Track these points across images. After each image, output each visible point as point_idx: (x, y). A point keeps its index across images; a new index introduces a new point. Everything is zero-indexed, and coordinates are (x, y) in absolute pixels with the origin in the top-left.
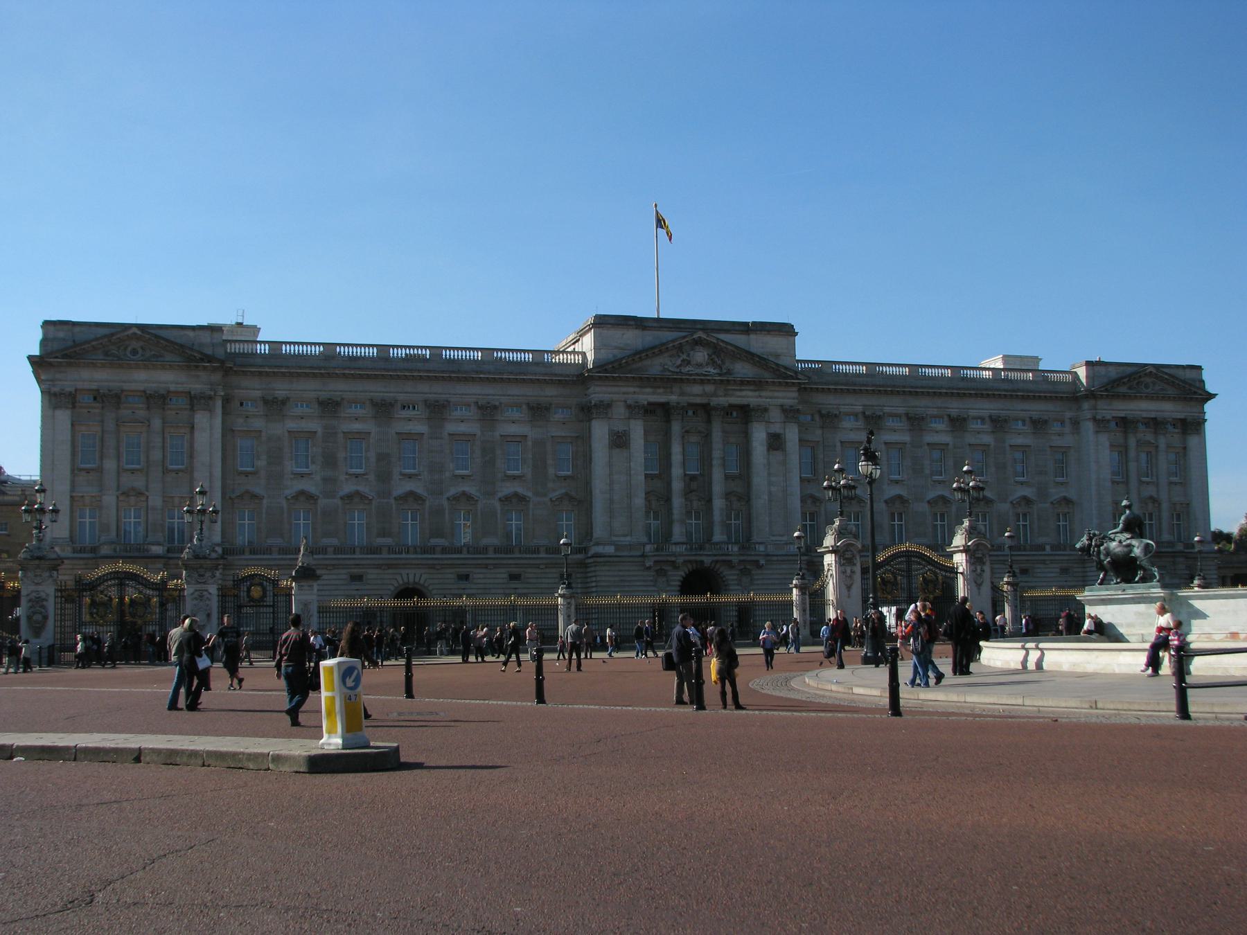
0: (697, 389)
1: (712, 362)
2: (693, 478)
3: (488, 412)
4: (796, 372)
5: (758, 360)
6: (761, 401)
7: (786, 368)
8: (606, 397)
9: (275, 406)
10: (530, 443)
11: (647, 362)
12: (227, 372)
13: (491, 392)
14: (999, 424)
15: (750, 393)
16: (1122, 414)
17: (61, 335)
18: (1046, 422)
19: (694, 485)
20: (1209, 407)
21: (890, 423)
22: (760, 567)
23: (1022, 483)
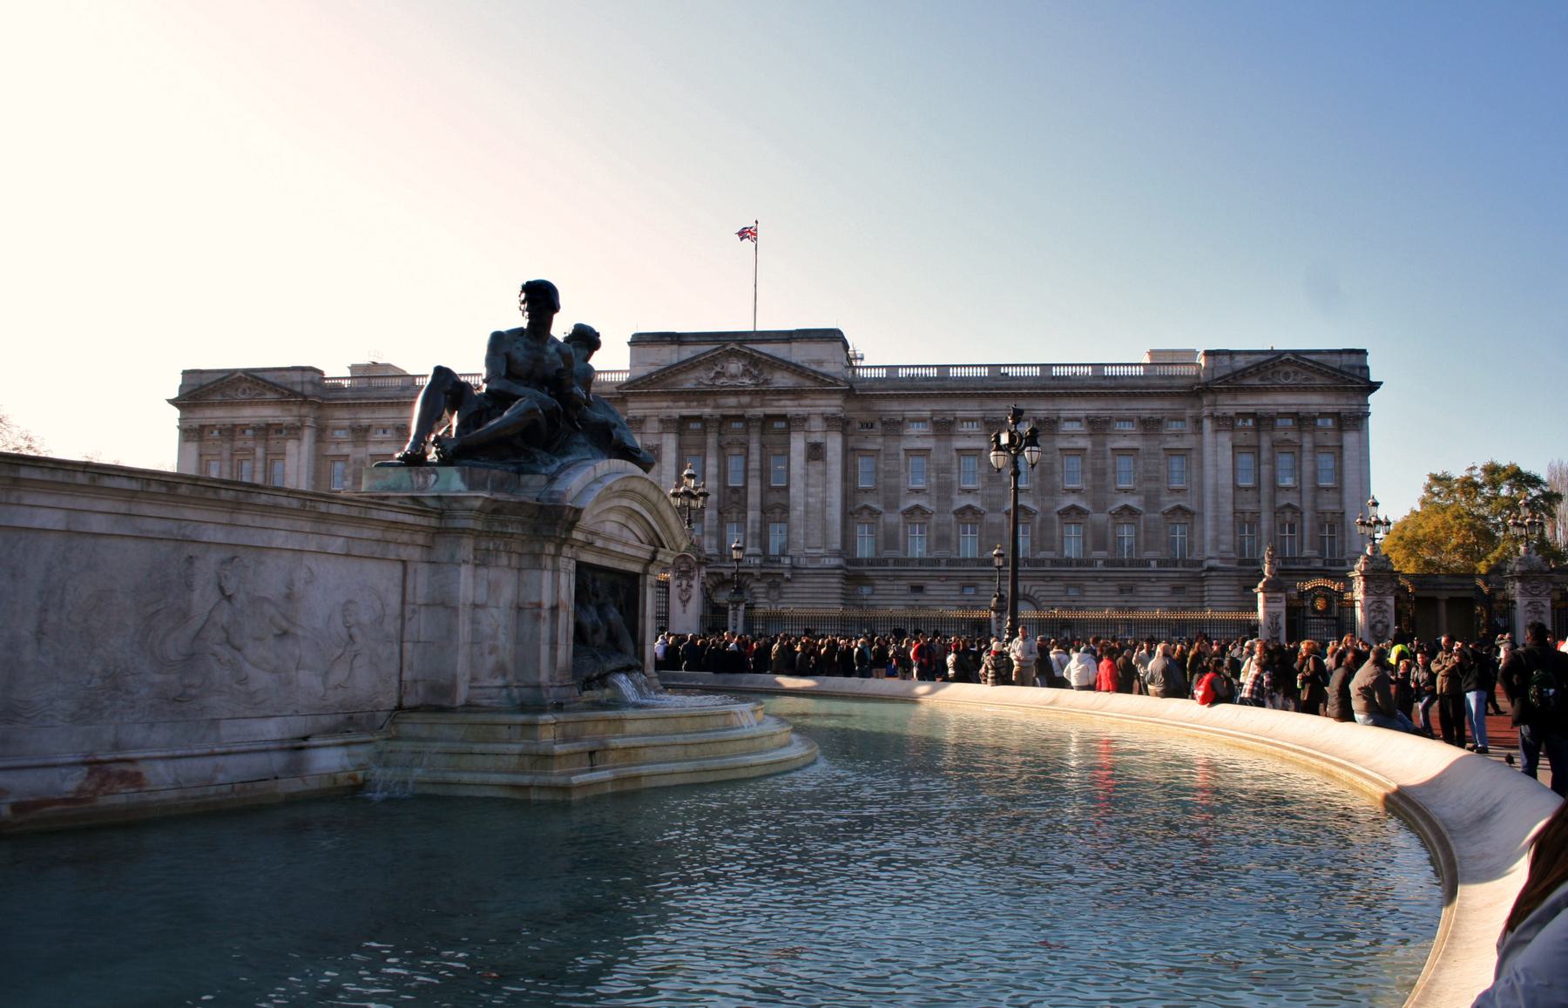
0: (732, 401)
1: (746, 373)
2: (735, 490)
6: (802, 411)
7: (824, 375)
8: (639, 413)
9: (360, 433)
11: (682, 377)
12: (320, 406)
15: (788, 403)
17: (194, 381)
18: (1159, 422)
19: (735, 498)
20: (1372, 398)
21: (966, 428)
22: (788, 580)
23: (1126, 491)
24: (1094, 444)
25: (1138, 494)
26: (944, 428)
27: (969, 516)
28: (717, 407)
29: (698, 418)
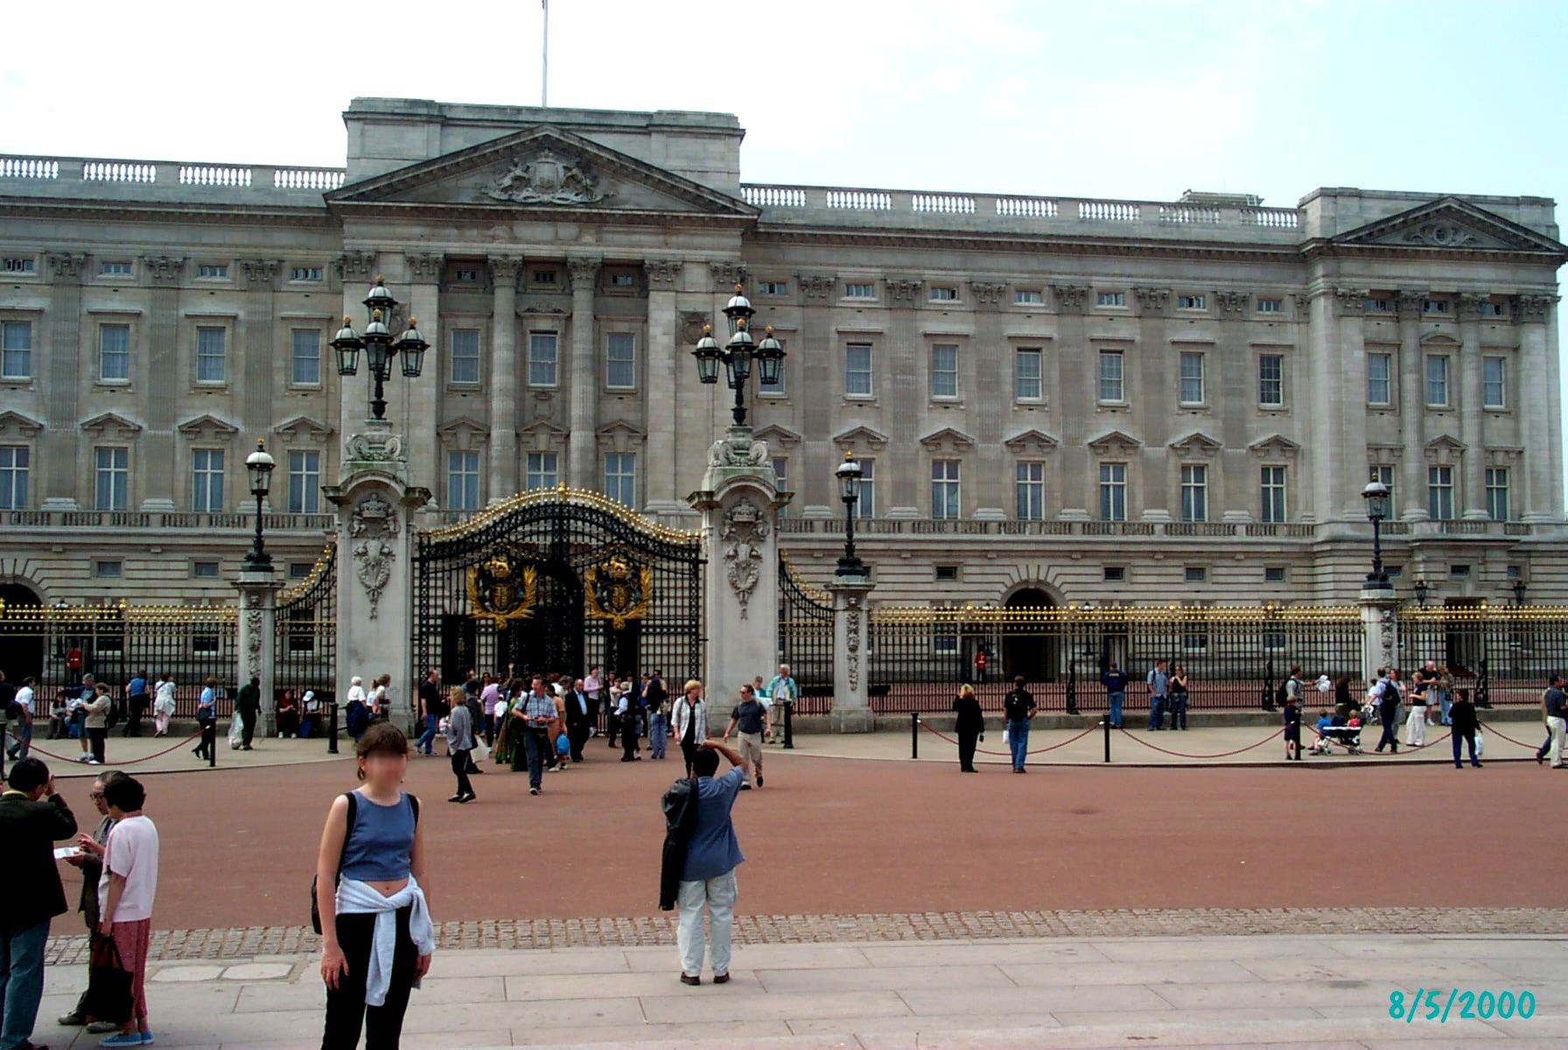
0: (543, 231)
1: (570, 182)
2: (543, 395)
3: (166, 272)
4: (733, 201)
5: (663, 181)
7: (713, 192)
8: (367, 245)
10: (242, 330)
11: (449, 183)
13: (173, 239)
14: (1150, 302)
15: (645, 238)
16: (1391, 285)
18: (1245, 300)
19: (543, 409)
24: (1142, 334)
25: (1214, 416)
26: (904, 294)
27: (947, 447)
28: (515, 239)
29: (482, 261)
